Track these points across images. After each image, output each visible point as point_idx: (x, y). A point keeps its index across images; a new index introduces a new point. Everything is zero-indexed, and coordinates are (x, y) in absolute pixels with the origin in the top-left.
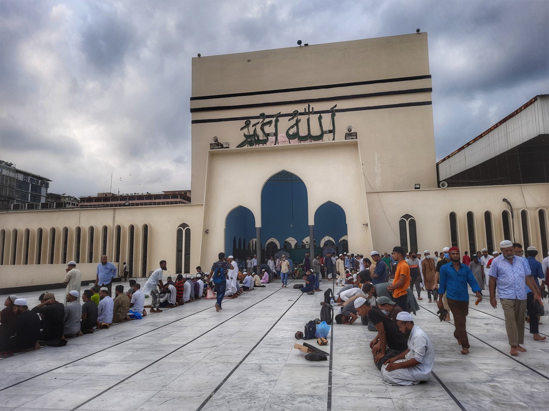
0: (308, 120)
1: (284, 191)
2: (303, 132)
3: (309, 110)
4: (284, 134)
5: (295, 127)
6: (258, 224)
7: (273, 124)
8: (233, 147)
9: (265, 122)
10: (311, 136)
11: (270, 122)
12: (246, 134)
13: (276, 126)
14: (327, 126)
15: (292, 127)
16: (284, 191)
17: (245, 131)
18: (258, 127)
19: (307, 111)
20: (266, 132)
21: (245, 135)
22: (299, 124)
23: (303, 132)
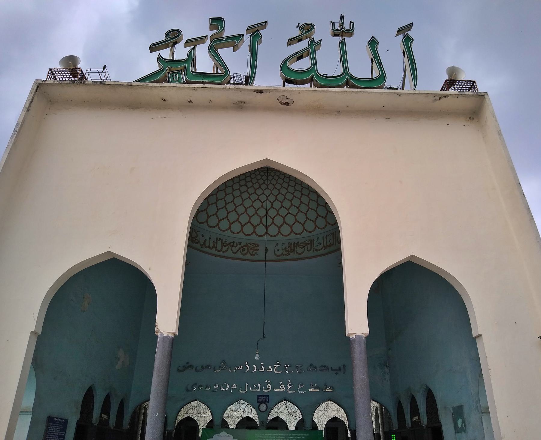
3: (342, 25)
6: (167, 320)
10: (352, 77)
19: (337, 27)
21: (160, 58)
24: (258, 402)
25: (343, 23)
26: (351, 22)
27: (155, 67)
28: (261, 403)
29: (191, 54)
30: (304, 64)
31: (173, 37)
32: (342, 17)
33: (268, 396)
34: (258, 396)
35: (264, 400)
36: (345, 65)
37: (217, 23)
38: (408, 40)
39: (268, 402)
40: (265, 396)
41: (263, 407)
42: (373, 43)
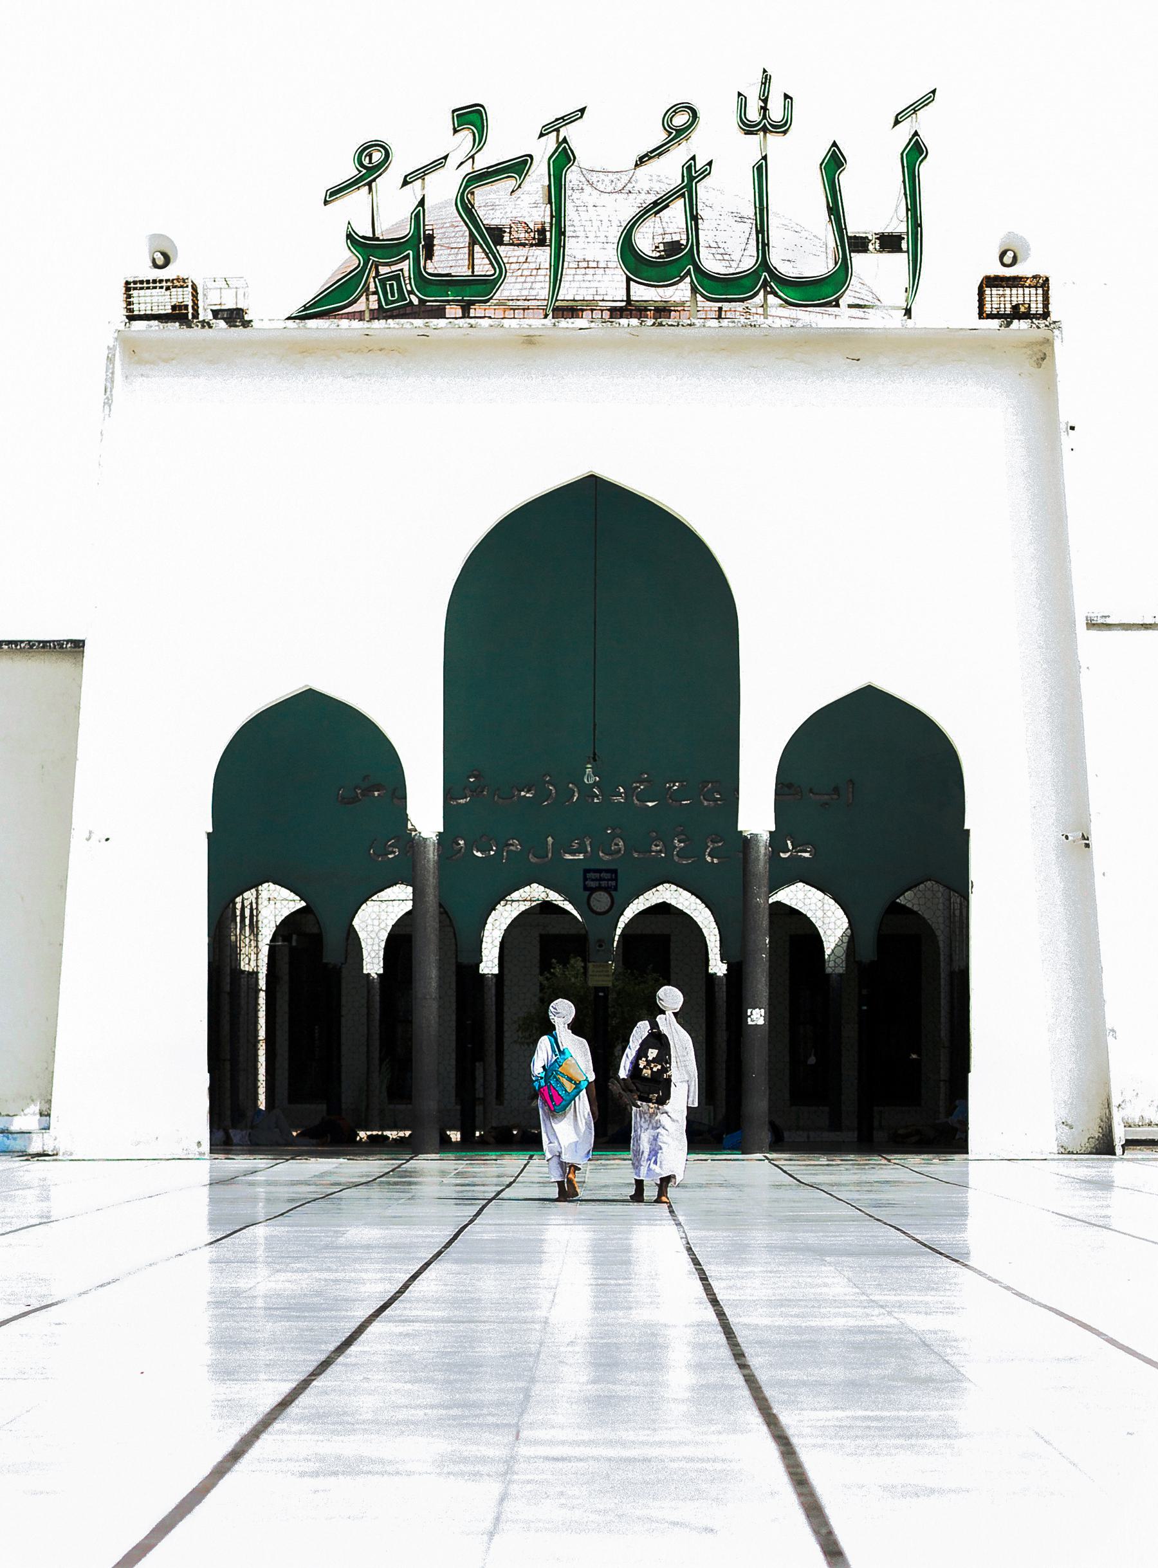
0: (761, 170)
1: (593, 604)
2: (726, 248)
3: (764, 109)
4: (611, 254)
5: (678, 206)
6: (426, 813)
7: (539, 174)
8: (272, 304)
9: (484, 160)
11: (519, 167)
12: (364, 230)
13: (556, 194)
14: (873, 206)
15: (658, 206)
16: (593, 604)
17: (355, 210)
18: (442, 189)
19: (753, 115)
20: (489, 217)
22: (703, 190)
23: (726, 248)
24: (586, 888)
25: (765, 101)
26: (786, 96)
27: (343, 259)
28: (592, 890)
29: (417, 218)
30: (674, 220)
31: (371, 163)
32: (766, 80)
33: (615, 872)
34: (586, 871)
35: (604, 883)
36: (764, 246)
37: (471, 118)
38: (916, 151)
39: (616, 889)
40: (607, 871)
41: (601, 900)
42: (834, 162)
